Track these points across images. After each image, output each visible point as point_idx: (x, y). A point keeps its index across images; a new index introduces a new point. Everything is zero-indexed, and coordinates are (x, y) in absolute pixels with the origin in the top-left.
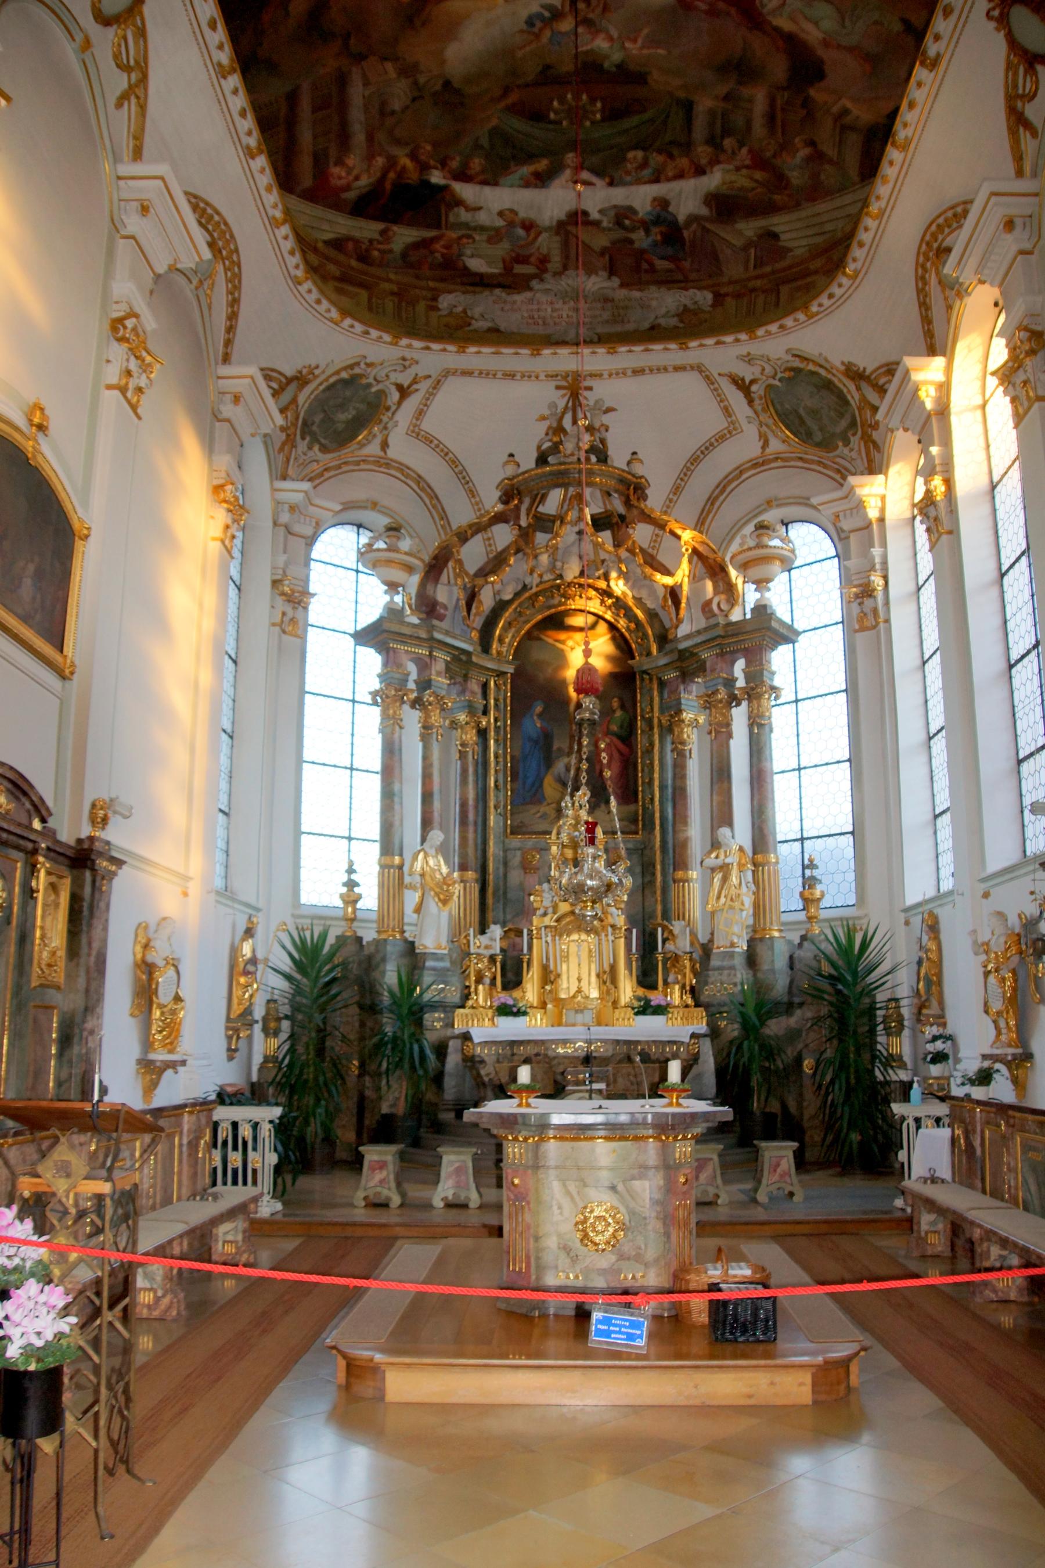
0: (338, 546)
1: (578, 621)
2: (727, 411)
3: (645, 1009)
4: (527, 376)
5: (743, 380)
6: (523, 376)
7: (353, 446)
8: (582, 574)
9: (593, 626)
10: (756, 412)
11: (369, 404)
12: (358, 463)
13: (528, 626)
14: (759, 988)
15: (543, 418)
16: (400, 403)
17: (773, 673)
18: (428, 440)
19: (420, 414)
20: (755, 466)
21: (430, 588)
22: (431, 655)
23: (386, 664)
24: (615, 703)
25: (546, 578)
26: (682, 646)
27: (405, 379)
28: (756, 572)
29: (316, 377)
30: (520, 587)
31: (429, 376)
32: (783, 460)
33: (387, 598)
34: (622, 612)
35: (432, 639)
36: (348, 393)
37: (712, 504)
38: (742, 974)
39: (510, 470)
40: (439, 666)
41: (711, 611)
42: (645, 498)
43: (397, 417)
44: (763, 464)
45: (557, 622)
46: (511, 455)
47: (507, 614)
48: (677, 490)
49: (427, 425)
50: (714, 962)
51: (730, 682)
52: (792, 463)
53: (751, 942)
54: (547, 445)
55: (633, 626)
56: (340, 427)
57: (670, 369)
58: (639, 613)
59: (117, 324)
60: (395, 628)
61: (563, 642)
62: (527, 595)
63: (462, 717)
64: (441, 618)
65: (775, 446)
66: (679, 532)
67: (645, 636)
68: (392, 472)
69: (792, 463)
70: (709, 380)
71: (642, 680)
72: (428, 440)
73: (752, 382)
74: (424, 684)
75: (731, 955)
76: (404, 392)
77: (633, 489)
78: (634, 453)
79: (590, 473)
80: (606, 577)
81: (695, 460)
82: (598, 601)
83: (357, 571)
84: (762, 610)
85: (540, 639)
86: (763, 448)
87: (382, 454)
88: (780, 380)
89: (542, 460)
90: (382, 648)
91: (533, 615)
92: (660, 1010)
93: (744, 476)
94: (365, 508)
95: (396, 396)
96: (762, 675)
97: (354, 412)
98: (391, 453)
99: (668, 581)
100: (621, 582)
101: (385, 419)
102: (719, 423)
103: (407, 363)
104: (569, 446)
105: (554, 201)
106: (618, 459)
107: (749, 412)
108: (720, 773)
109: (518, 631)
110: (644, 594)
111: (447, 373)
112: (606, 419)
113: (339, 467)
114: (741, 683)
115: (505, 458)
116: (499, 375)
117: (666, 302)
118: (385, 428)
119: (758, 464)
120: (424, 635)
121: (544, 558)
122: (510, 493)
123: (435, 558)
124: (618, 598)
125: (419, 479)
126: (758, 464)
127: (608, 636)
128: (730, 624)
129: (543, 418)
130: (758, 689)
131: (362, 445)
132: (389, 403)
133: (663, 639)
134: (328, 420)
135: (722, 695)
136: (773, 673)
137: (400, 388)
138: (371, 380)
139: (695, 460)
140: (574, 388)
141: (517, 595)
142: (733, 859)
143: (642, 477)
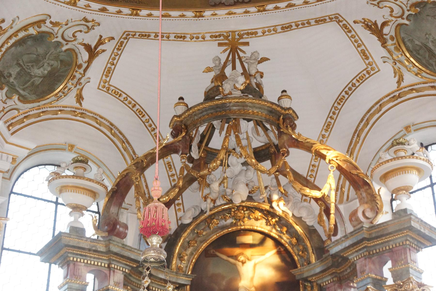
0: (35, 180)
1: (249, 239)
2: (365, 55)
4: (195, 37)
5: (375, 24)
6: (192, 38)
7: (51, 97)
8: (250, 198)
9: (262, 243)
10: (389, 52)
11: (62, 61)
12: (56, 113)
13: (205, 245)
15: (209, 70)
16: (89, 62)
17: (421, 273)
18: (118, 94)
19: (108, 72)
20: (395, 98)
21: (113, 210)
22: (109, 267)
25: (218, 203)
26: (334, 250)
27: (91, 39)
28: (395, 182)
29: (5, 31)
30: (197, 213)
31: (113, 38)
32: (417, 90)
33: (72, 219)
34: (285, 229)
35: (109, 252)
36: (41, 50)
37: (358, 136)
39: (181, 110)
40: (119, 276)
41: (358, 219)
42: (294, 127)
43: (89, 74)
44: (399, 96)
45: (230, 240)
46: (181, 98)
47: (185, 235)
49: (116, 81)
52: (426, 92)
55: (294, 240)
56: (38, 81)
57: (313, 22)
58: (298, 228)
60: (74, 241)
61: (236, 257)
62: (203, 217)
65: (410, 79)
66: (324, 152)
67: (305, 249)
68: (87, 120)
69: (426, 92)
70: (346, 28)
71: (305, 287)
72: (118, 94)
73: (384, 24)
76: (93, 52)
77: (282, 119)
78: (284, 91)
79: (244, 105)
80: (270, 201)
81: (341, 100)
82: (264, 221)
83: (57, 203)
85: (217, 256)
86: (399, 82)
87: (78, 105)
88: (407, 19)
90: (65, 262)
91: (209, 235)
93: (384, 109)
94: (64, 150)
95: (85, 56)
96: (408, 271)
97: (49, 69)
98: (86, 105)
99: (317, 194)
100: (282, 203)
101: (78, 76)
102: (361, 65)
103: (90, 24)
104: (227, 87)
106: (271, 94)
107: (384, 53)
109: (196, 250)
110: (303, 214)
111: (128, 35)
112: (261, 67)
113: (39, 115)
114: (390, 282)
115: (177, 101)
116: (172, 37)
118: (79, 83)
119: (396, 97)
120: (102, 248)
121: (215, 186)
122: (181, 127)
123: (118, 185)
124: (280, 218)
125: (111, 126)
126: (396, 97)
127: (275, 251)
128: (373, 227)
129: (209, 70)
131: (59, 98)
132: (80, 61)
133: (321, 250)
134: (24, 74)
136: (421, 273)
137: (88, 47)
138: (60, 39)
139: (341, 100)
140: (233, 44)
141: (195, 219)
143: (290, 109)
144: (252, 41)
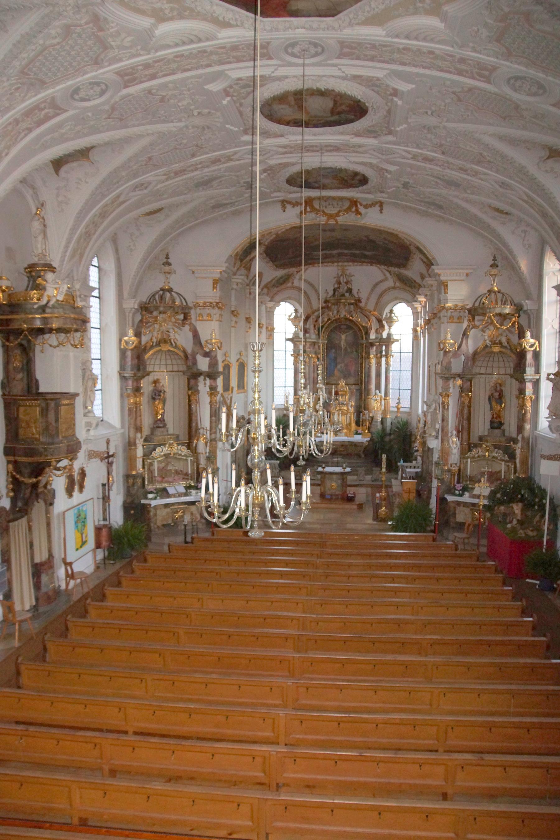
2: (385, 275)
3: (357, 433)
14: (384, 429)
23: (295, 347)
24: (354, 350)
38: (379, 426)
48: (372, 290)
50: (373, 423)
51: (381, 352)
53: (382, 419)
54: (336, 286)
59: (247, 318)
63: (314, 356)
64: (308, 333)
74: (305, 351)
75: (377, 422)
76: (297, 272)
81: (377, 284)
84: (389, 335)
89: (335, 290)
92: (359, 434)
98: (295, 284)
105: (335, 252)
108: (378, 375)
112: (352, 278)
114: (384, 353)
117: (366, 260)
119: (394, 288)
122: (326, 301)
130: (387, 356)
135: (379, 355)
139: (377, 284)
142: (378, 399)
144: (349, 268)
